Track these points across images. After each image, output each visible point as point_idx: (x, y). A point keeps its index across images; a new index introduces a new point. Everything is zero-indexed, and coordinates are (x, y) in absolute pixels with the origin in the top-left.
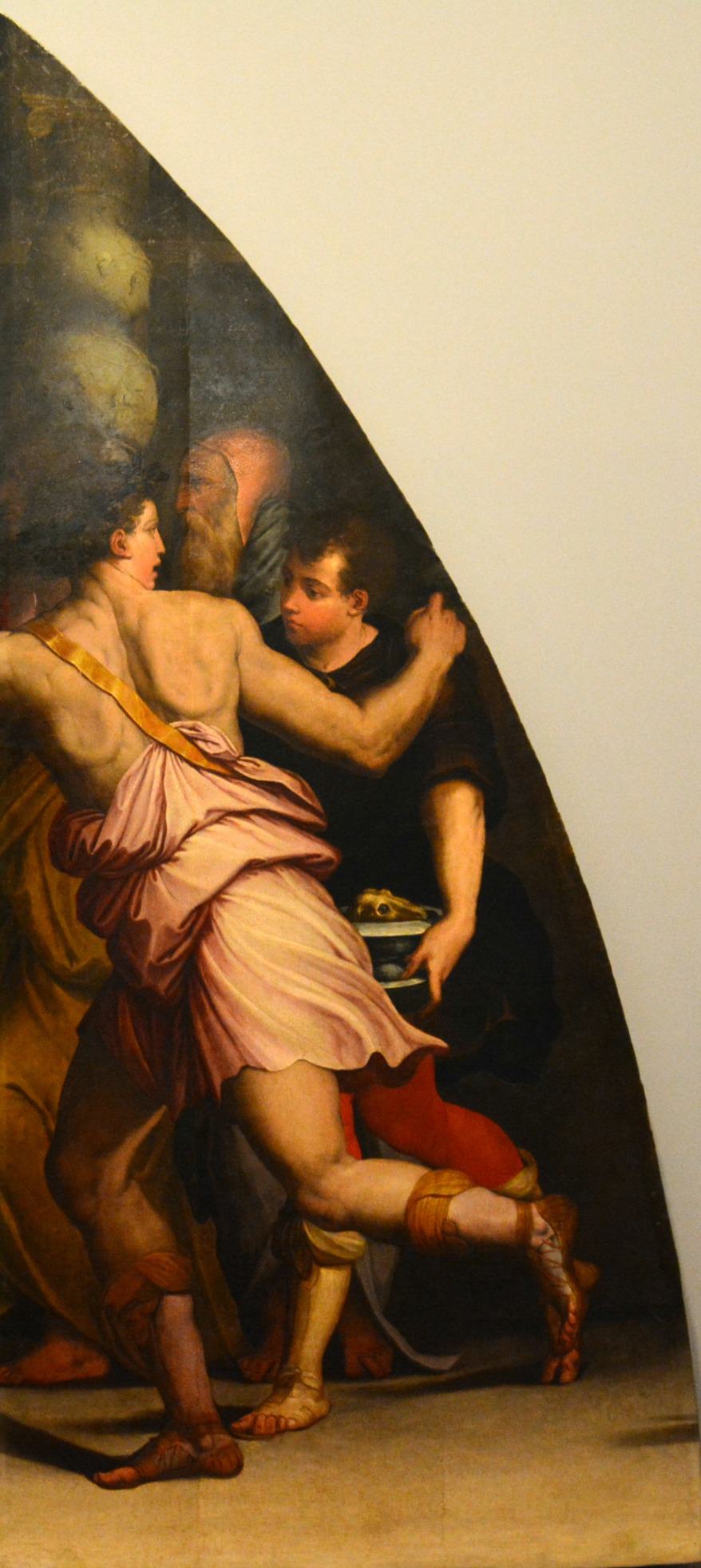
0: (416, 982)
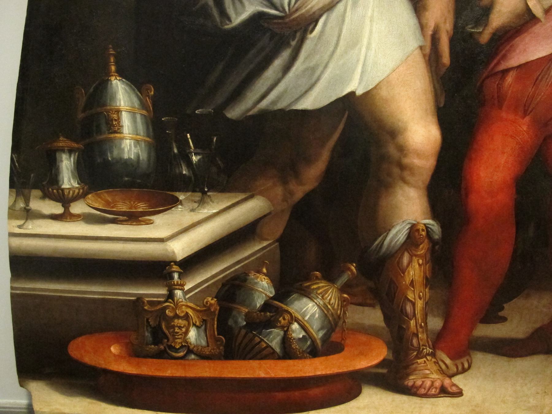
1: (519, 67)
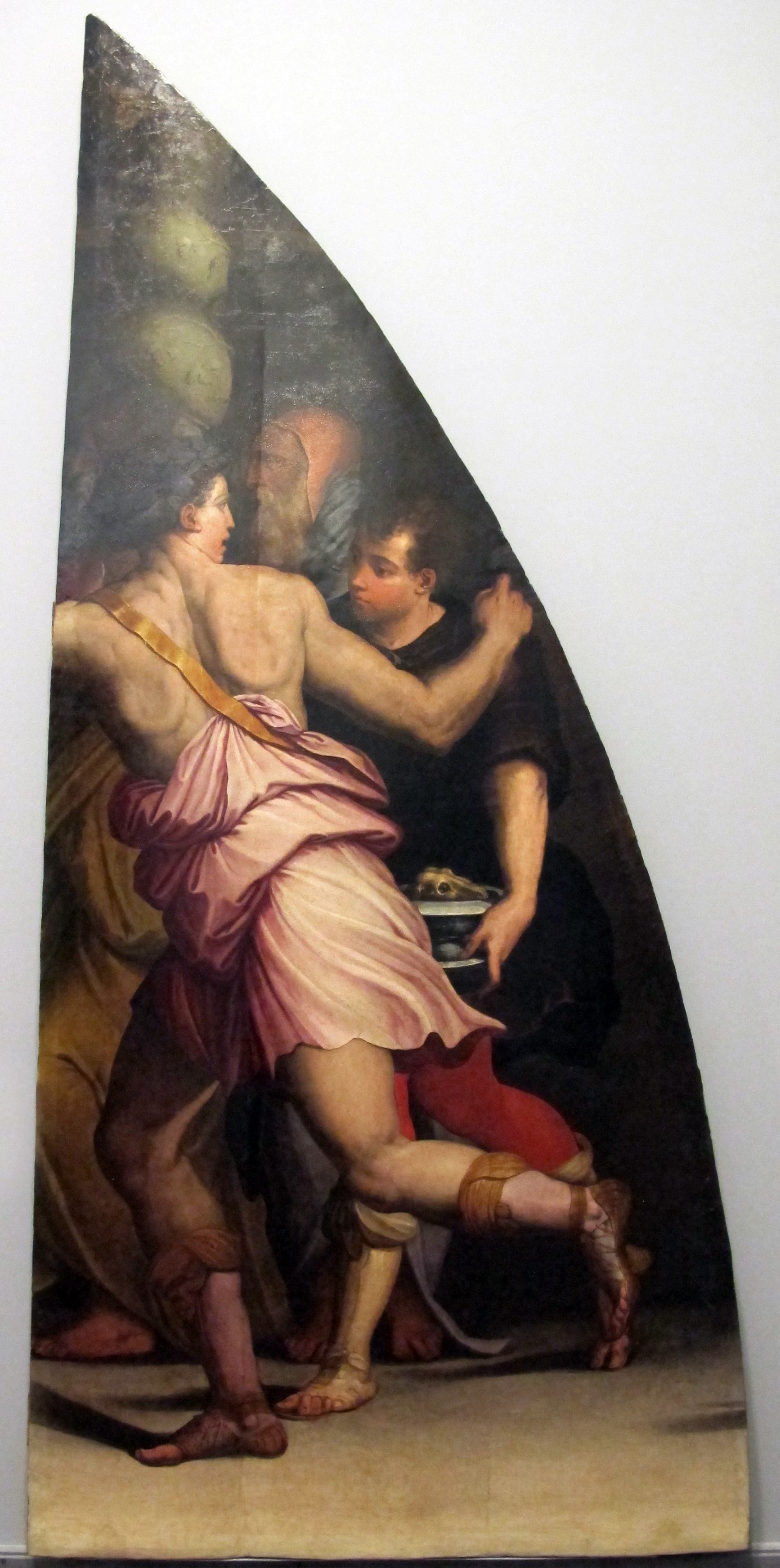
0: (474, 962)
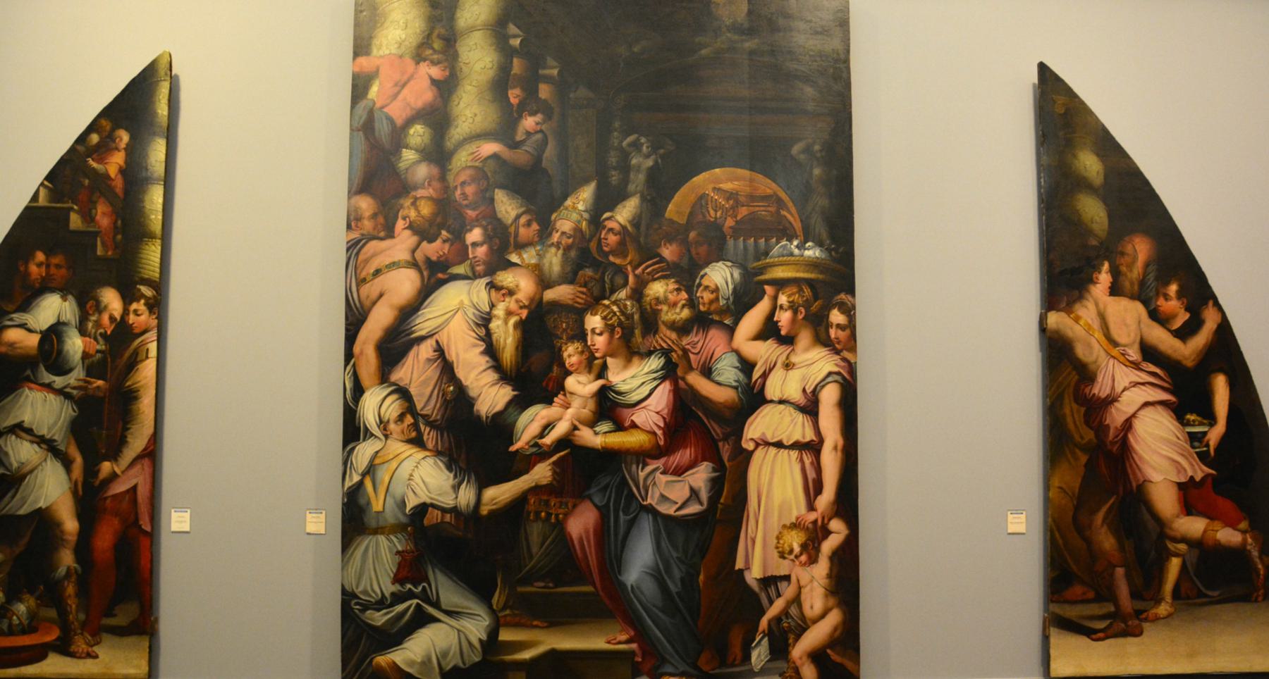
0: (1205, 449)
1: (113, 496)
